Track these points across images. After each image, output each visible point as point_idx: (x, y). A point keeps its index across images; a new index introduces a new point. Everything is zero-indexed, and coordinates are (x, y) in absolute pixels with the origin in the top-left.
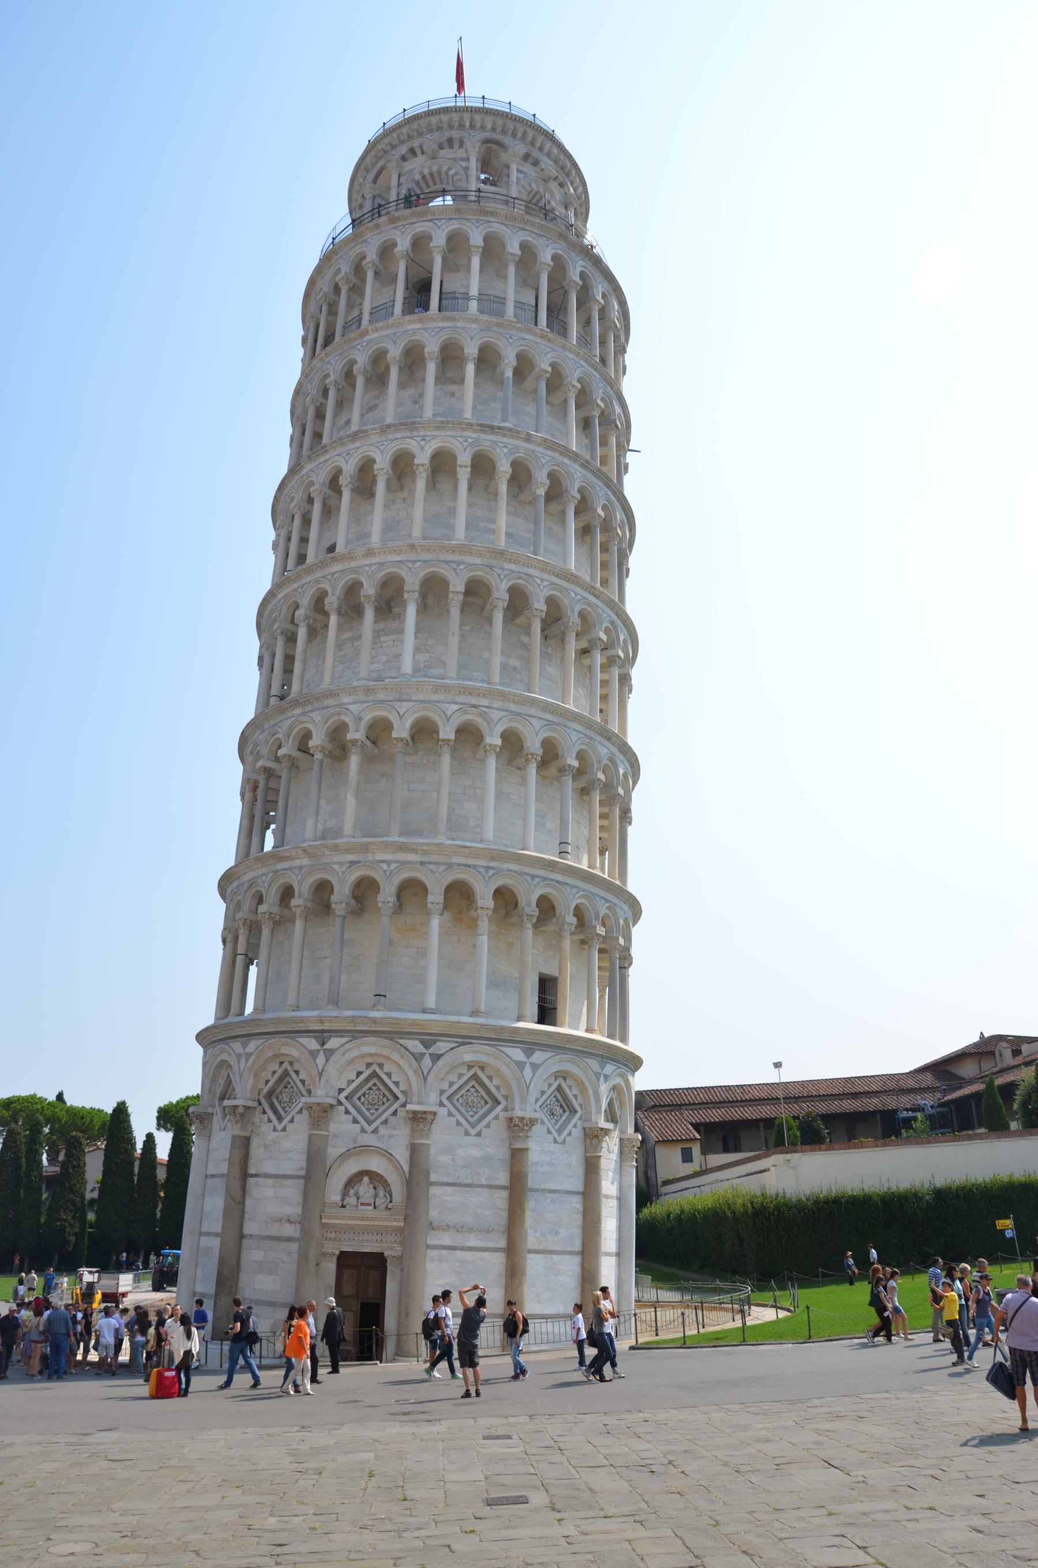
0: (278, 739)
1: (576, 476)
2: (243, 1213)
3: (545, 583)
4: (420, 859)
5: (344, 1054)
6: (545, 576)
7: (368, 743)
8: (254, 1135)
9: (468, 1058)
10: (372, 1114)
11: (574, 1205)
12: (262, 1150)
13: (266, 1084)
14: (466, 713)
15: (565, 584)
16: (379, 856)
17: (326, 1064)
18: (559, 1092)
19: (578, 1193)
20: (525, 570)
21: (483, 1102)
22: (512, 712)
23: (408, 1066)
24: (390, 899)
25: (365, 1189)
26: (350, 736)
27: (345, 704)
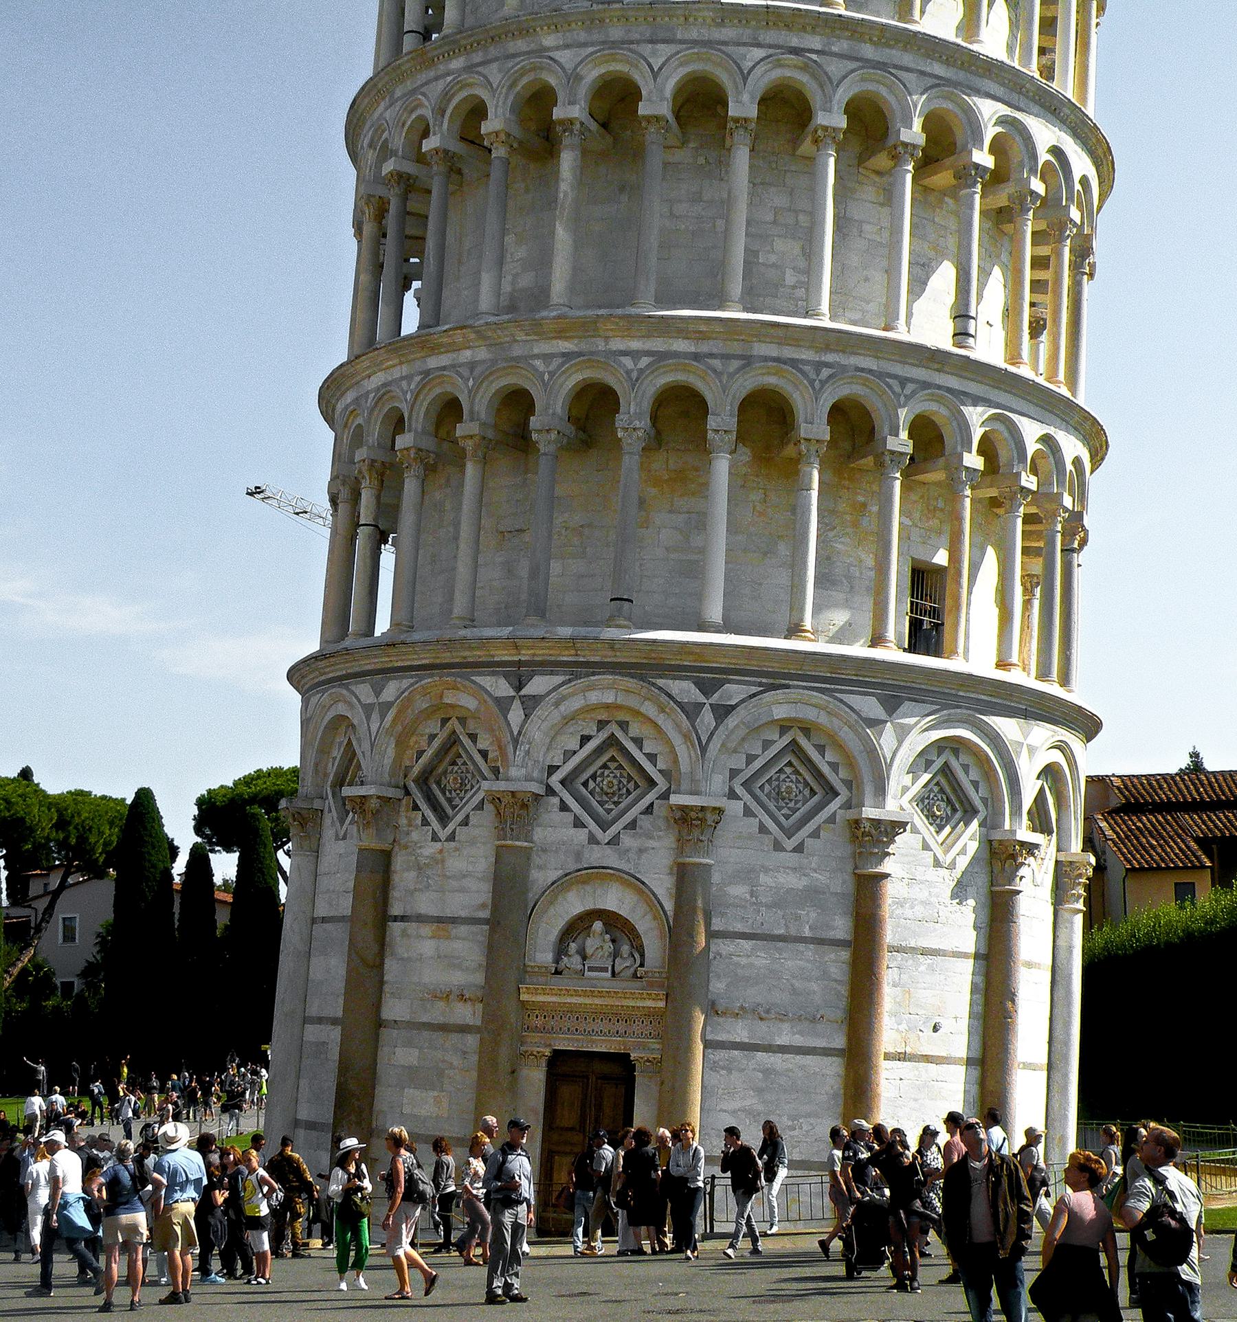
0: (422, 118)
2: (382, 982)
4: (693, 349)
5: (557, 704)
7: (594, 126)
8: (396, 849)
9: (780, 712)
10: (609, 811)
12: (412, 874)
13: (418, 759)
14: (779, 64)
16: (617, 344)
17: (525, 721)
18: (946, 776)
21: (807, 792)
22: (867, 61)
24: (637, 424)
25: (597, 941)
26: (558, 113)
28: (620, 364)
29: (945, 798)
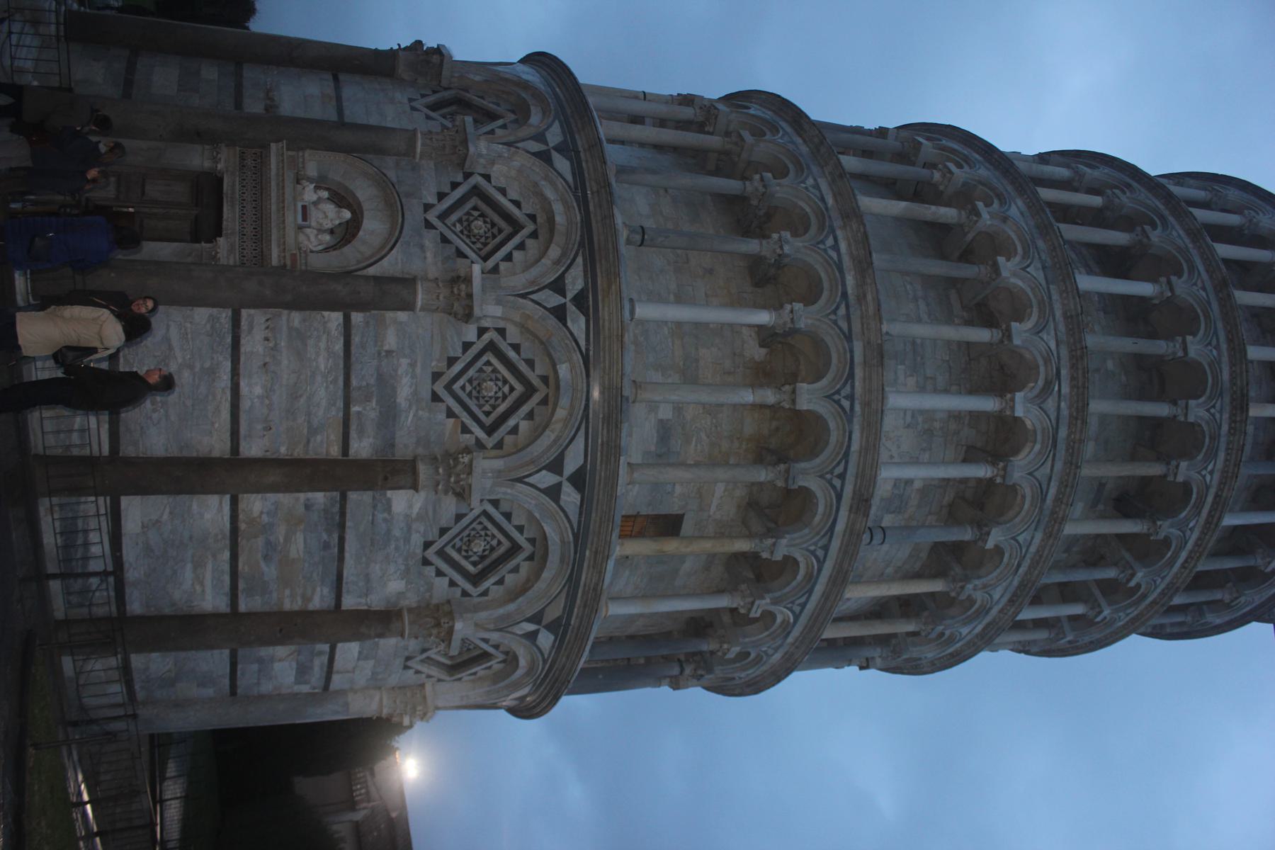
3: (1208, 478)
4: (850, 291)
5: (546, 178)
6: (1216, 476)
7: (970, 237)
9: (563, 370)
11: (318, 589)
13: (478, 97)
14: (1047, 361)
16: (839, 233)
17: (528, 152)
20: (1223, 446)
21: (487, 408)
22: (1057, 433)
23: (546, 270)
24: (787, 249)
25: (331, 215)
27: (1016, 204)
28: (827, 237)
29: (486, 553)
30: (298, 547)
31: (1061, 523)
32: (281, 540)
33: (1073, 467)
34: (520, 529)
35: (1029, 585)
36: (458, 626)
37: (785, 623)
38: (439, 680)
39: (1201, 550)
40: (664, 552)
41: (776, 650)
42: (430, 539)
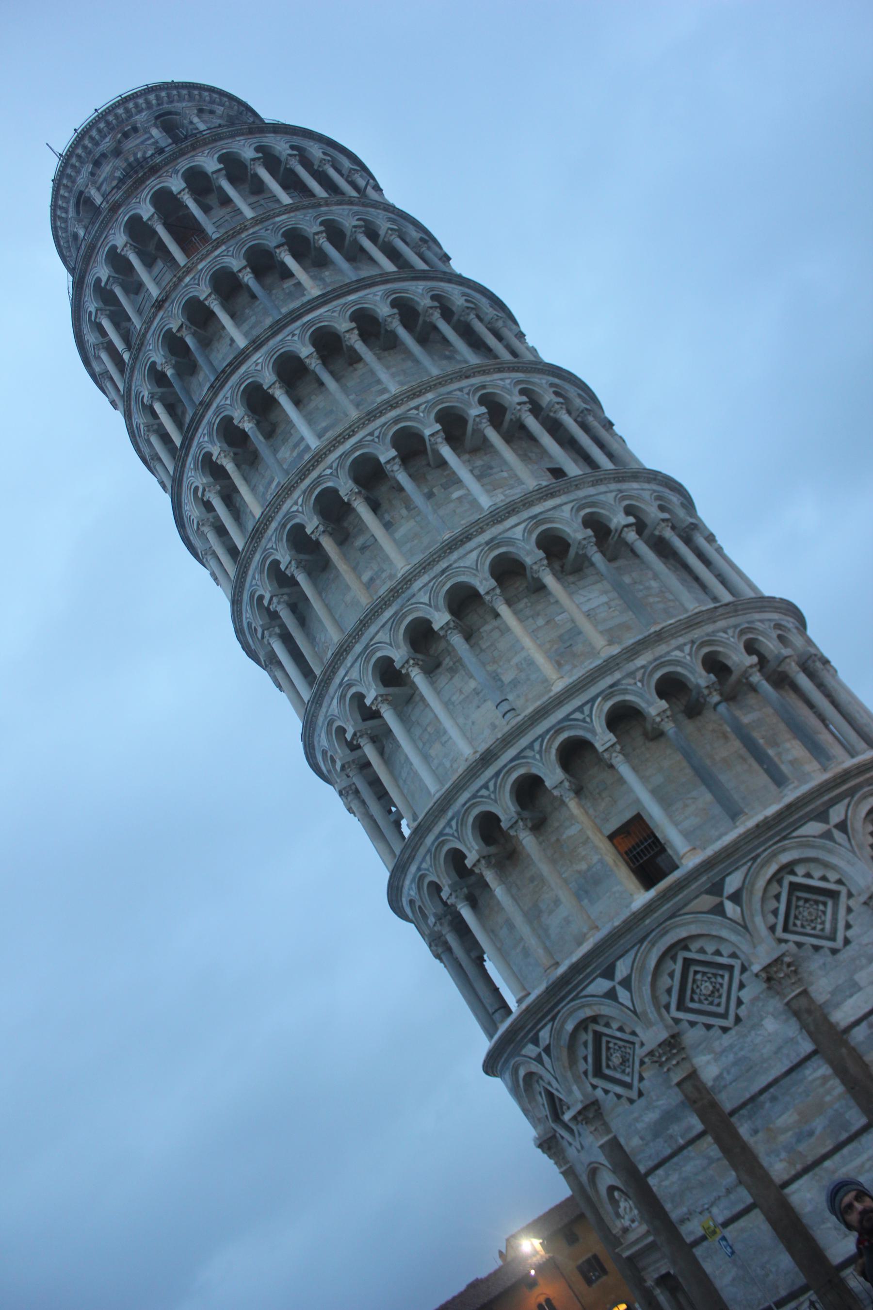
1: (259, 368)
6: (297, 493)
9: (570, 1027)
11: (810, 1078)
15: (314, 474)
19: (808, 1057)
30: (787, 1119)
31: (395, 588)
32: (790, 1133)
33: (364, 622)
34: (671, 975)
35: (446, 548)
36: (756, 968)
37: (606, 699)
38: (850, 895)
39: (334, 442)
40: (615, 861)
41: (631, 674)
42: (720, 1032)
